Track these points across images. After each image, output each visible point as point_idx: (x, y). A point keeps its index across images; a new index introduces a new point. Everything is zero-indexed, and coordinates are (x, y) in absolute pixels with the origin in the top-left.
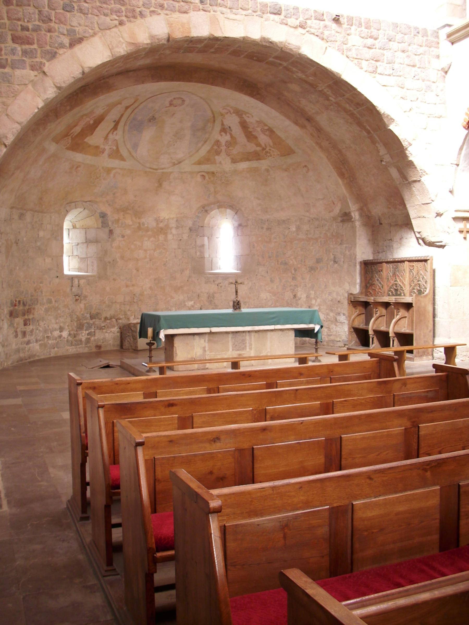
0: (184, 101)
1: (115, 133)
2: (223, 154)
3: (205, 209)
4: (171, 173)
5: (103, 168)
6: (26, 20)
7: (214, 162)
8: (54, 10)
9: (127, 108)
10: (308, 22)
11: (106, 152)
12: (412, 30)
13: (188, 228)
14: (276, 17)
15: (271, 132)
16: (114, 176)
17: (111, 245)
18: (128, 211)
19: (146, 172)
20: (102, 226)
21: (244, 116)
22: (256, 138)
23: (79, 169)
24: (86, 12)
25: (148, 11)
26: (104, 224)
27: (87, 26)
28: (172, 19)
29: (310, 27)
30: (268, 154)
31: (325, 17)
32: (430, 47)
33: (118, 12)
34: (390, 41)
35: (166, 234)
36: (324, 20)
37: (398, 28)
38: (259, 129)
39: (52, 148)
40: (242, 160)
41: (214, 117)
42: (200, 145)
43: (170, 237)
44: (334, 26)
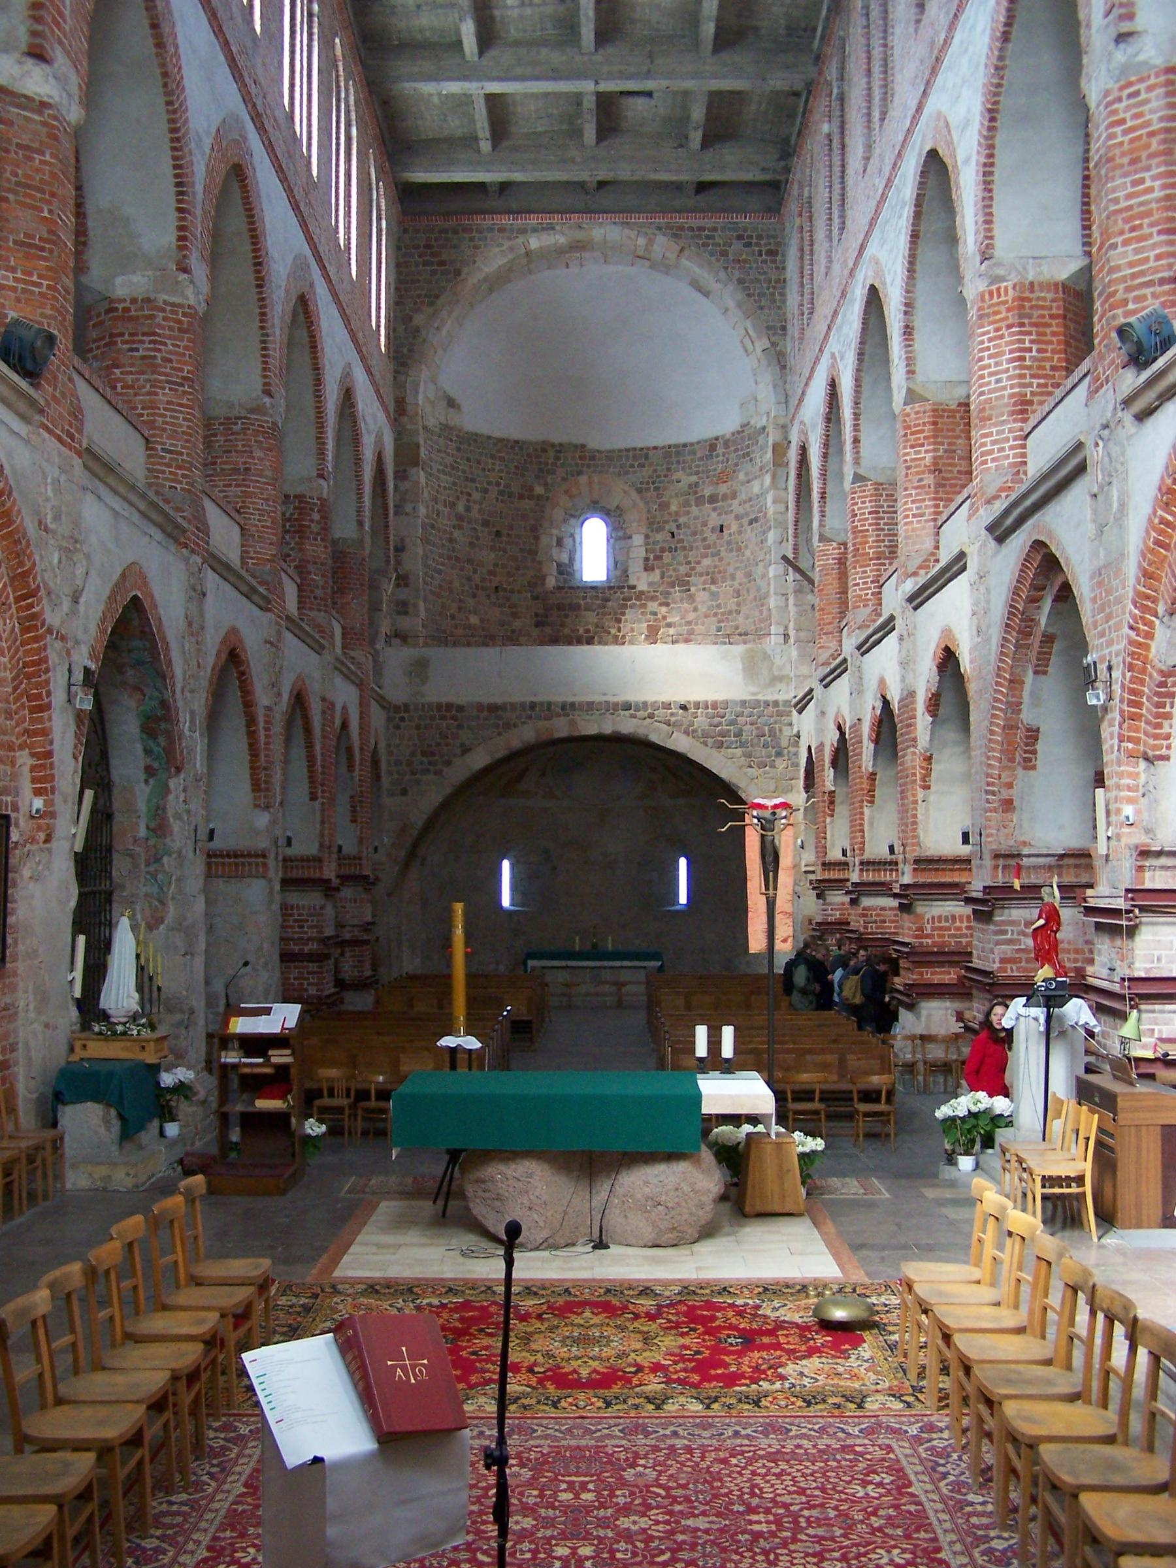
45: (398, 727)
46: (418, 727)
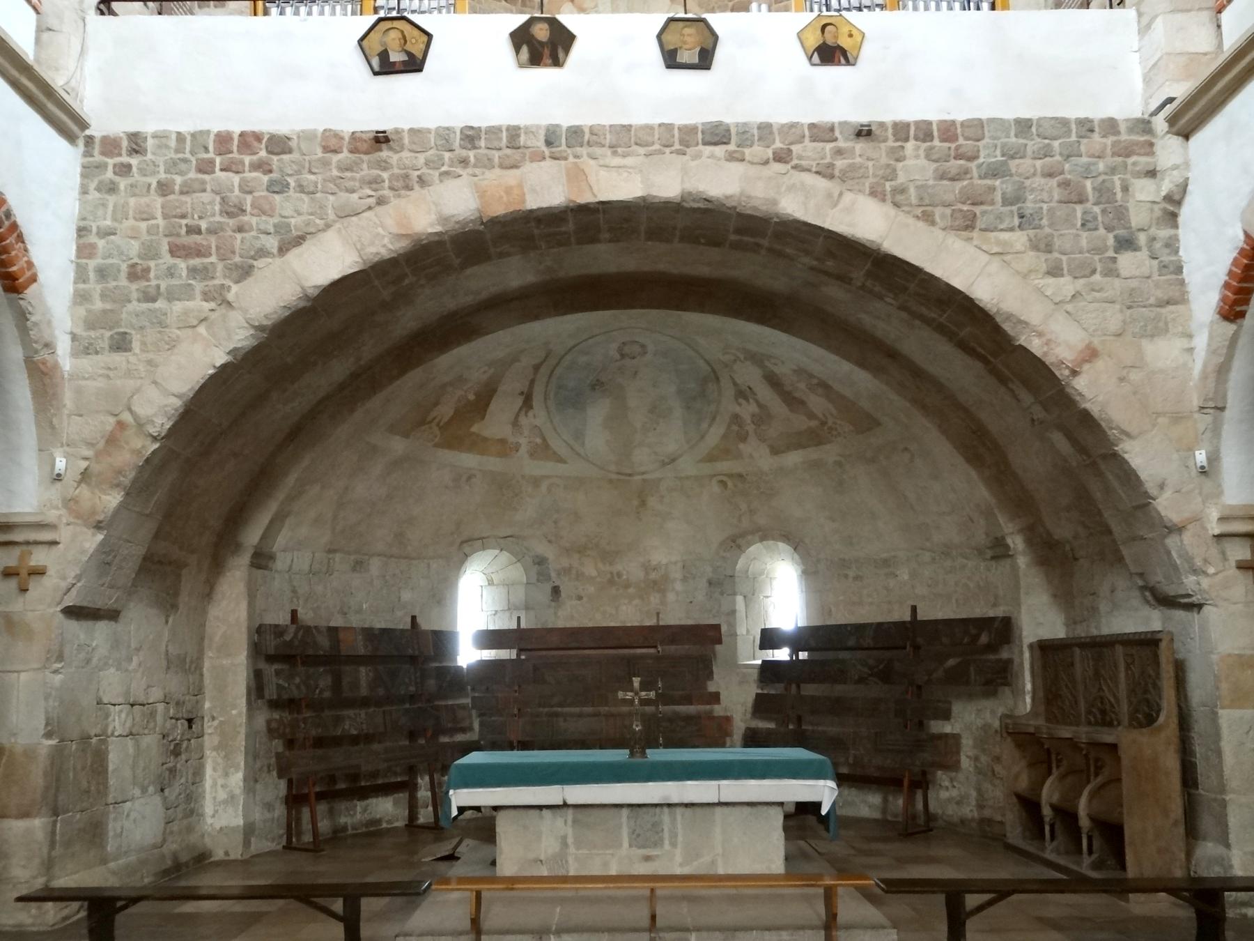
0: (643, 346)
1: (530, 414)
2: (752, 439)
3: (736, 543)
4: (660, 480)
5: (523, 477)
6: (196, 216)
7: (739, 456)
8: (250, 192)
9: (537, 368)
10: (794, 148)
11: (523, 450)
12: (1073, 127)
13: (705, 580)
14: (719, 150)
15: (824, 387)
16: (549, 490)
17: (555, 613)
18: (589, 552)
19: (611, 481)
20: (538, 580)
21: (767, 363)
22: (802, 403)
23: (474, 480)
24: (312, 189)
25: (436, 173)
26: (543, 576)
27: (311, 214)
28: (486, 182)
29: (800, 158)
30: (834, 433)
31: (837, 134)
32: (1128, 156)
33: (375, 182)
34: (1012, 157)
35: (663, 592)
36: (836, 140)
37: (1034, 129)
38: (802, 386)
39: (398, 445)
40: (790, 447)
41: (714, 371)
42: (705, 425)
43: (671, 597)
44: (860, 146)
45: (112, 189)
46: (164, 188)
